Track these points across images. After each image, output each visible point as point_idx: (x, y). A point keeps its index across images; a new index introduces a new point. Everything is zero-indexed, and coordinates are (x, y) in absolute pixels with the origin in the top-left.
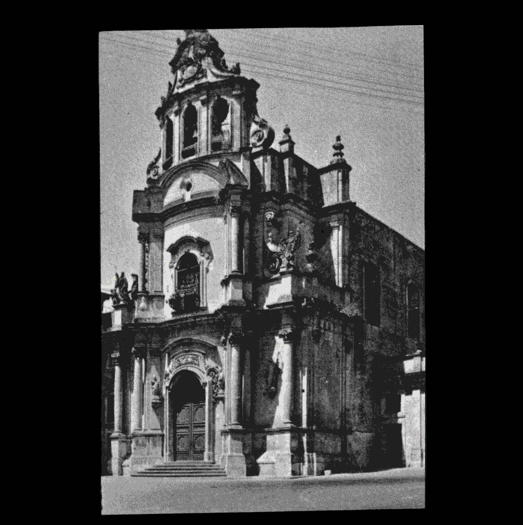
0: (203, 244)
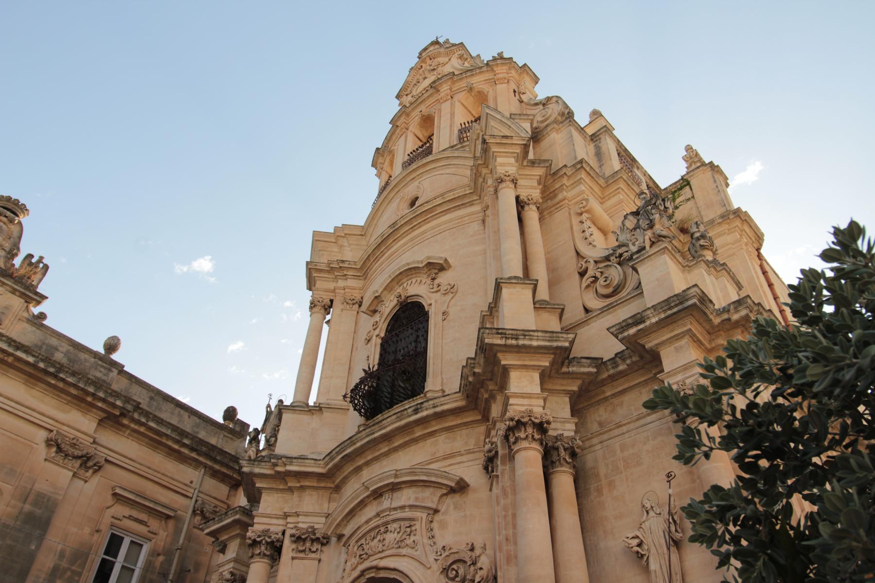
0: (436, 268)
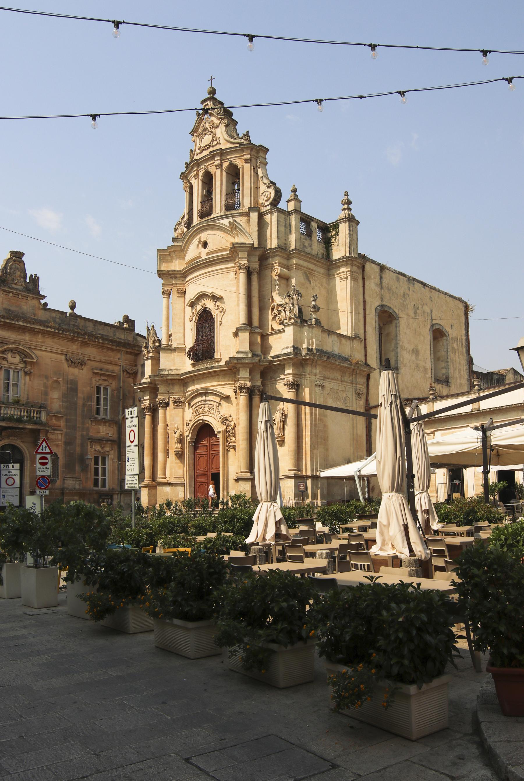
0: (216, 298)
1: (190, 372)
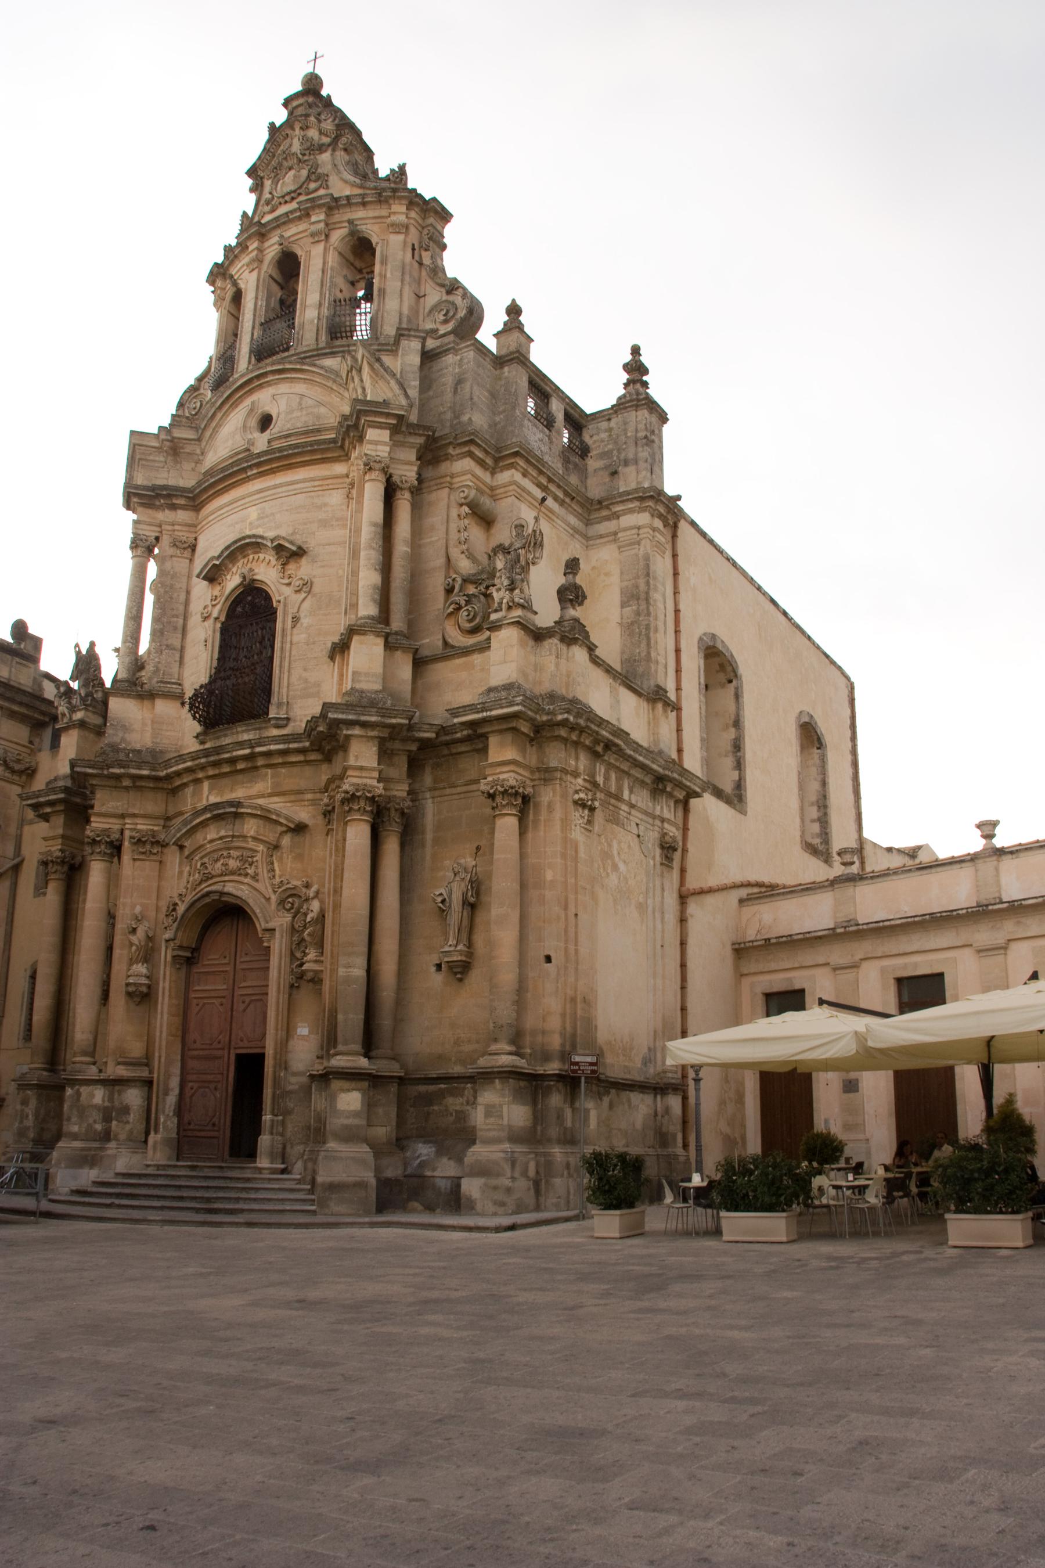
0: (290, 554)
1: (194, 755)
